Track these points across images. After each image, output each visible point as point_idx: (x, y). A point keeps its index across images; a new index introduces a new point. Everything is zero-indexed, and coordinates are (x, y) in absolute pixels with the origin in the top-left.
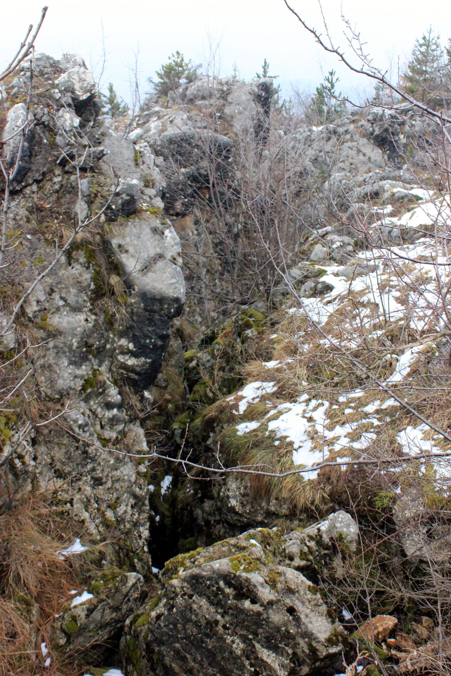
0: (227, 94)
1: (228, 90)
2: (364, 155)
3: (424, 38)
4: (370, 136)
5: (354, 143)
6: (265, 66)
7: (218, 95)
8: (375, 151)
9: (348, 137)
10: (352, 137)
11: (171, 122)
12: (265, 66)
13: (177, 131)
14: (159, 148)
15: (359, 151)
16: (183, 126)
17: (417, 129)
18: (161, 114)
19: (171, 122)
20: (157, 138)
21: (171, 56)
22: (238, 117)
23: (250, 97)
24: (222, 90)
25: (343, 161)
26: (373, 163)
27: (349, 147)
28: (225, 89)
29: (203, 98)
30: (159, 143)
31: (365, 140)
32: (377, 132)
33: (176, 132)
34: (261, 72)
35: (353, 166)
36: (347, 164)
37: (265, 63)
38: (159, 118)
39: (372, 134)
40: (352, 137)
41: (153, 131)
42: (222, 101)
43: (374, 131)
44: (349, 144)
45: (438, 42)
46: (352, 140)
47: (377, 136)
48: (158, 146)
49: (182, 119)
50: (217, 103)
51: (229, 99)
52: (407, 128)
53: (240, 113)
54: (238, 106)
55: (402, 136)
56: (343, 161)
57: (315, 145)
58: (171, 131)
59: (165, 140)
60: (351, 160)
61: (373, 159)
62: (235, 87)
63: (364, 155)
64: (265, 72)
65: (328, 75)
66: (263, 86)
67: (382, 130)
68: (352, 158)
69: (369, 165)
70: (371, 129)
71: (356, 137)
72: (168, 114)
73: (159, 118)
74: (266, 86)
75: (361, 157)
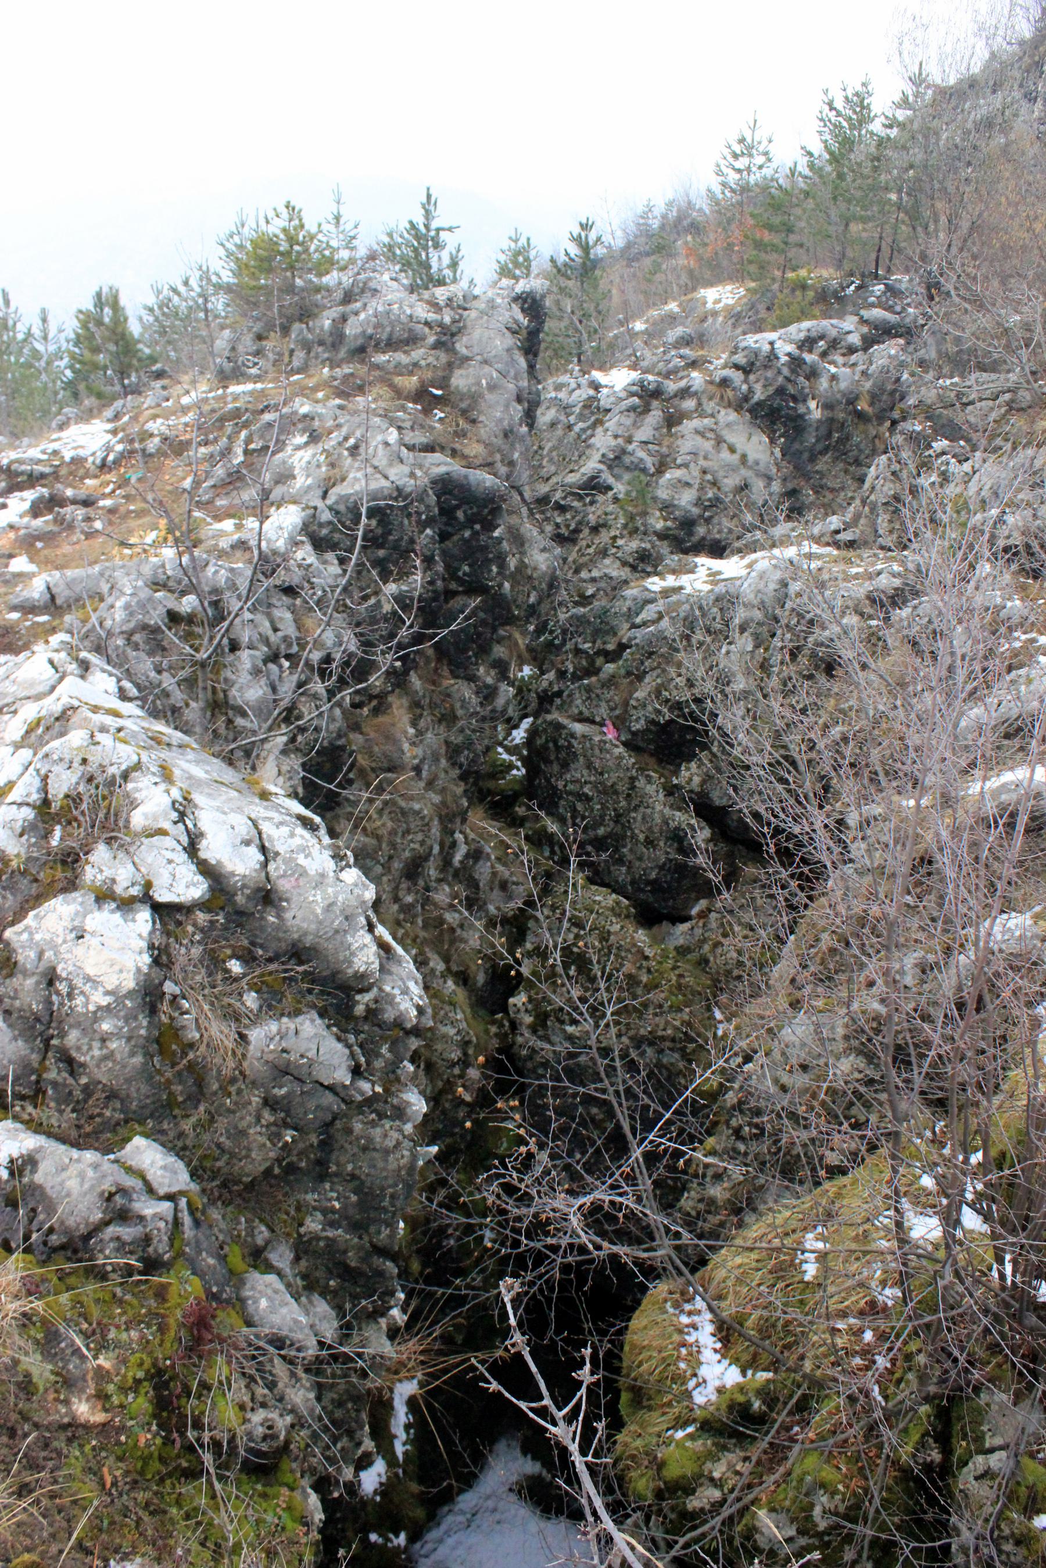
0: (453, 335)
1: (454, 322)
2: (732, 450)
3: (742, 141)
4: (741, 403)
5: (706, 421)
6: (429, 205)
7: (431, 339)
8: (755, 439)
9: (689, 404)
10: (700, 404)
11: (354, 450)
12: (429, 205)
13: (379, 484)
14: (324, 532)
15: (719, 441)
16: (391, 465)
17: (843, 385)
18: (316, 423)
19: (354, 450)
20: (320, 504)
21: (271, 214)
22: (489, 396)
23: (510, 340)
24: (441, 325)
25: (686, 465)
26: (750, 468)
27: (697, 432)
28: (447, 320)
29: (392, 344)
30: (326, 516)
31: (732, 416)
32: (759, 395)
33: (374, 486)
34: (420, 221)
35: (709, 477)
36: (695, 471)
37: (429, 197)
38: (314, 438)
39: (746, 399)
40: (700, 404)
41: (301, 481)
42: (444, 357)
43: (750, 390)
44: (695, 423)
45: (771, 148)
46: (700, 411)
47: (759, 404)
48: (321, 525)
49: (387, 444)
50: (430, 359)
51: (461, 347)
52: (824, 383)
53: (492, 387)
54: (487, 369)
55: (812, 404)
56: (686, 465)
57: (612, 423)
58: (358, 483)
59: (342, 508)
60: (702, 462)
61: (751, 457)
62: (473, 314)
63: (732, 450)
64: (428, 215)
65: (576, 230)
66: (525, 301)
67: (771, 390)
68: (705, 458)
69: (744, 472)
70: (745, 387)
71: (710, 406)
72: (339, 426)
73: (314, 438)
74: (534, 300)
75: (725, 455)
